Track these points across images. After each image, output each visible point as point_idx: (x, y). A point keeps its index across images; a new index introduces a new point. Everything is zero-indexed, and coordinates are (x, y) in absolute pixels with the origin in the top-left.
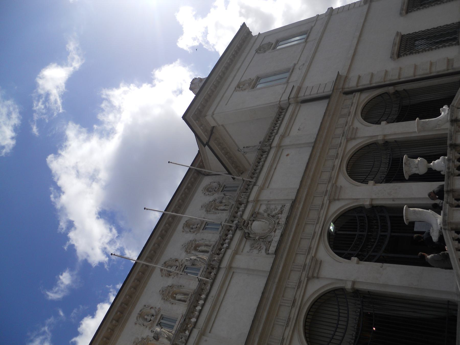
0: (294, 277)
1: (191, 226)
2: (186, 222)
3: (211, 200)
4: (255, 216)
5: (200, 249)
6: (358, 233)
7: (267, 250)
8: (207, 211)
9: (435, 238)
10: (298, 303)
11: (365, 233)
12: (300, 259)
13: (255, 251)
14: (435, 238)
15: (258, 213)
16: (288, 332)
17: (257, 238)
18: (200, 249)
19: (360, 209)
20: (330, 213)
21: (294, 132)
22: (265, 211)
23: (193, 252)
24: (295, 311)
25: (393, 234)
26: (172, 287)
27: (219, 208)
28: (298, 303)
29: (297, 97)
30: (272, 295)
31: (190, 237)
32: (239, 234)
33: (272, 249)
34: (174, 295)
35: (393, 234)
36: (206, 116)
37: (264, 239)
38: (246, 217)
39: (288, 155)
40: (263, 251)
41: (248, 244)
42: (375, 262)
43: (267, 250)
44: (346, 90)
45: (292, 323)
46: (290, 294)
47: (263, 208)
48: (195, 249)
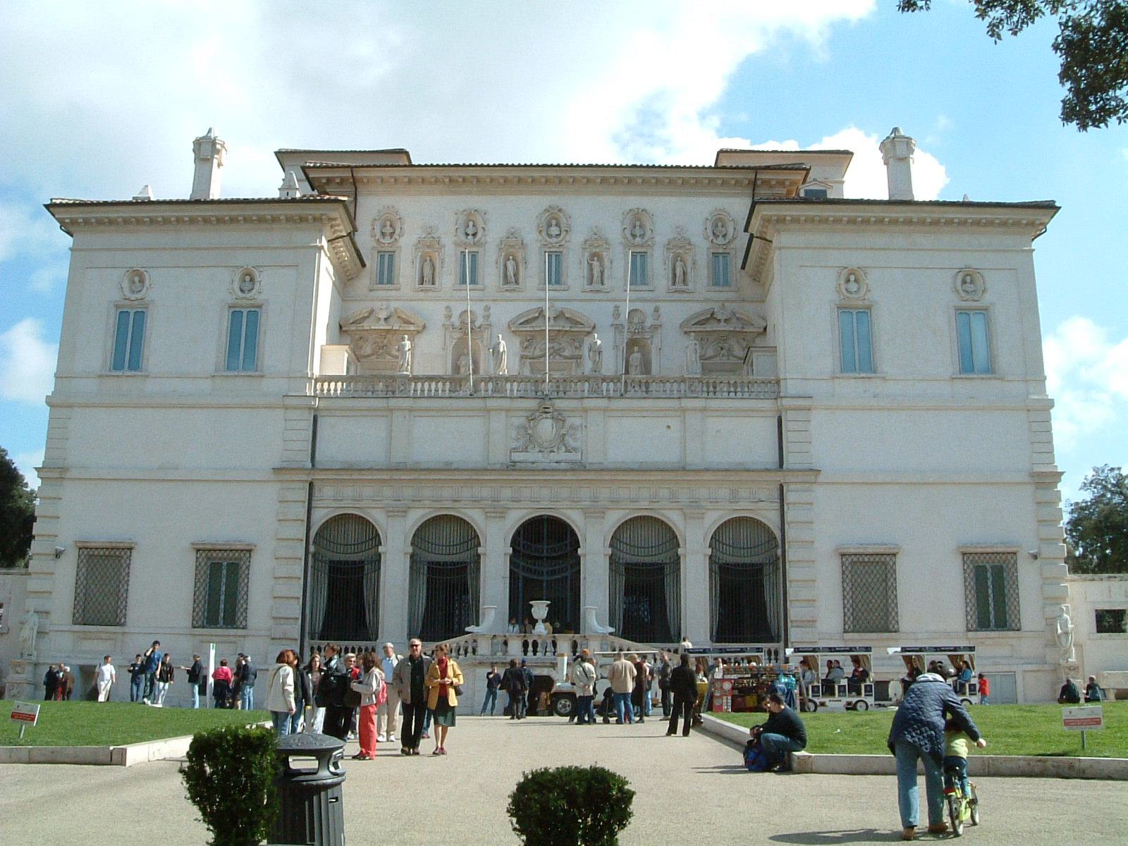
0: (486, 492)
1: (638, 223)
3: (693, 240)
4: (559, 418)
5: (596, 263)
7: (515, 450)
8: (669, 246)
9: (467, 629)
10: (457, 505)
11: (545, 554)
12: (507, 493)
13: (514, 434)
14: (467, 629)
17: (530, 432)
18: (596, 263)
19: (576, 544)
20: (569, 512)
21: (714, 423)
22: (572, 427)
23: (587, 254)
26: (523, 245)
27: (678, 264)
29: (787, 410)
30: (457, 477)
31: (614, 231)
32: (533, 404)
33: (517, 457)
34: (511, 257)
36: (778, 231)
37: (530, 440)
38: (559, 404)
39: (669, 427)
40: (514, 445)
41: (523, 420)
42: (510, 569)
43: (515, 450)
46: (466, 493)
47: (577, 421)
48: (594, 256)
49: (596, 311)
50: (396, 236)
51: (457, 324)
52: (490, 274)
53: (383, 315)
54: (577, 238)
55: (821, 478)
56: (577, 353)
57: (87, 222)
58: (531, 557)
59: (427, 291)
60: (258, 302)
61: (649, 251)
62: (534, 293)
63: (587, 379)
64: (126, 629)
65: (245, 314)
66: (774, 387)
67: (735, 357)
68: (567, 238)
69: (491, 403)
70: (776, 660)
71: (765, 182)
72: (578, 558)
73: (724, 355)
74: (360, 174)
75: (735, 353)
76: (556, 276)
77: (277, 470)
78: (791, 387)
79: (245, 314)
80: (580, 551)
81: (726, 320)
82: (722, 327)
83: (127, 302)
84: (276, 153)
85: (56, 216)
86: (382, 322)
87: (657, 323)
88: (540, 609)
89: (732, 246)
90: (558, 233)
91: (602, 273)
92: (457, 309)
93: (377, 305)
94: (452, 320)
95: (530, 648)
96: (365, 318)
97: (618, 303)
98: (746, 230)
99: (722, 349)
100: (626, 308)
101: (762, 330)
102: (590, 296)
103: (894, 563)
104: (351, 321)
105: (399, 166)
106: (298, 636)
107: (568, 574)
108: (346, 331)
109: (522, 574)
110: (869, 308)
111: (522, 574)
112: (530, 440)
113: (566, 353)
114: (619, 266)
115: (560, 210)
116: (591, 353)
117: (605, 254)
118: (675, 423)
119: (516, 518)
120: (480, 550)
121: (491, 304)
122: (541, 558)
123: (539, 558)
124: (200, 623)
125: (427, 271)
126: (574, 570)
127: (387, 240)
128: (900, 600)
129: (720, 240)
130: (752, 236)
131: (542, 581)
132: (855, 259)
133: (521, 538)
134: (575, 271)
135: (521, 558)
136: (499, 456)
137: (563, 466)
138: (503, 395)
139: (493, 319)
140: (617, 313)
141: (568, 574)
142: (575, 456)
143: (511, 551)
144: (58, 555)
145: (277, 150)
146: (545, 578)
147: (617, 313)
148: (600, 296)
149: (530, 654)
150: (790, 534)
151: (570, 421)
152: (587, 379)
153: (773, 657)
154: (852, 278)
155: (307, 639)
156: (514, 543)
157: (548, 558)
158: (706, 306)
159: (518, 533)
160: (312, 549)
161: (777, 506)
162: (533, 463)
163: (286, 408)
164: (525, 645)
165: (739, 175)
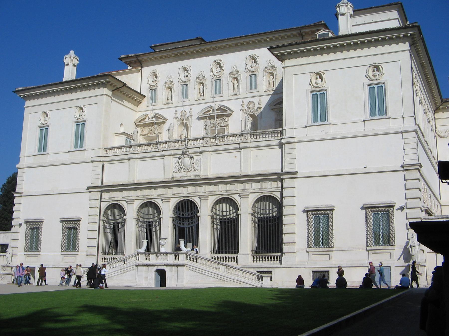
11: (186, 216)
13: (174, 165)
15: (193, 158)
16: (141, 197)
19: (198, 211)
24: (149, 197)
25: (186, 229)
33: (175, 175)
38: (190, 150)
39: (236, 157)
51: (179, 117)
53: (151, 117)
54: (226, 72)
55: (298, 175)
56: (226, 124)
61: (257, 73)
64: (41, 253)
65: (80, 125)
66: (282, 133)
69: (165, 153)
71: (307, 33)
72: (198, 217)
74: (140, 58)
76: (218, 90)
77: (89, 188)
78: (287, 134)
79: (80, 125)
83: (42, 125)
86: (151, 119)
91: (238, 86)
96: (145, 118)
100: (246, 101)
102: (233, 97)
103: (332, 214)
105: (215, 41)
106: (96, 254)
110: (326, 90)
112: (180, 166)
113: (222, 125)
115: (220, 60)
117: (238, 78)
118: (238, 154)
122: (185, 218)
123: (183, 218)
125: (170, 95)
127: (154, 84)
128: (334, 232)
132: (318, 68)
134: (227, 86)
136: (169, 176)
137: (192, 178)
141: (196, 223)
142: (196, 173)
143: (173, 215)
144: (20, 225)
148: (237, 97)
150: (286, 201)
151: (194, 157)
154: (318, 77)
155: (100, 254)
157: (187, 218)
160: (102, 218)
161: (280, 189)
163: (92, 162)
165: (294, 33)
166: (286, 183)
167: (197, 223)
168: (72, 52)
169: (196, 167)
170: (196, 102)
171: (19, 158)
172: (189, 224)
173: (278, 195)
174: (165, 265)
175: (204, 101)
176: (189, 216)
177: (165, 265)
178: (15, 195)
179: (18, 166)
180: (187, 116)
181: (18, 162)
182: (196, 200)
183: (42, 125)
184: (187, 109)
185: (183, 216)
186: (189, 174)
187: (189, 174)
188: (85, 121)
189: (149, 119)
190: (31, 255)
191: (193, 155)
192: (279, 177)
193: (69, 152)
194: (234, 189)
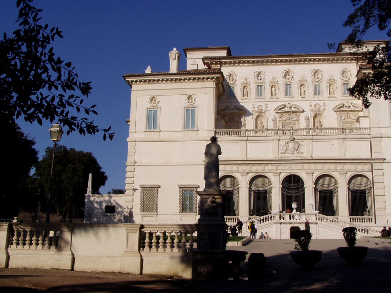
0: (273, 167)
2: (318, 69)
6: (293, 185)
7: (282, 153)
8: (328, 81)
10: (263, 171)
11: (293, 187)
23: (299, 85)
24: (261, 171)
25: (293, 197)
28: (263, 171)
32: (288, 138)
35: (293, 197)
39: (333, 145)
43: (282, 153)
44: (373, 164)
45: (257, 171)
48: (301, 85)
49: (304, 105)
50: (234, 81)
51: (257, 110)
52: (267, 92)
57: (136, 81)
58: (288, 188)
59: (246, 99)
60: (195, 106)
62: (282, 99)
63: (305, 129)
67: (352, 119)
68: (293, 80)
70: (372, 222)
73: (348, 118)
75: (352, 118)
80: (304, 186)
81: (349, 107)
82: (347, 109)
84: (184, 50)
85: (126, 80)
87: (325, 108)
88: (294, 205)
89: (349, 81)
90: (289, 78)
92: (257, 105)
93: (229, 104)
94: (255, 109)
95: (292, 218)
96: (226, 109)
97: (311, 102)
98: (356, 77)
99: (347, 116)
100: (313, 103)
101: (361, 110)
102: (301, 99)
104: (221, 110)
107: (301, 193)
108: (220, 114)
109: (285, 194)
111: (285, 194)
113: (294, 119)
114: (310, 88)
116: (306, 120)
119: (283, 175)
120: (272, 186)
121: (267, 103)
122: (292, 188)
124: (181, 211)
126: (302, 193)
129: (345, 79)
130: (358, 78)
131: (292, 196)
133: (285, 182)
135: (285, 189)
137: (298, 158)
138: (277, 135)
139: (268, 109)
140: (311, 105)
141: (301, 193)
143: (281, 186)
145: (184, 48)
146: (293, 195)
147: (311, 105)
148: (305, 99)
149: (292, 219)
152: (305, 129)
153: (370, 221)
156: (282, 183)
157: (294, 188)
158: (342, 102)
159: (284, 180)
162: (288, 157)
164: (290, 217)
166: (375, 166)
167: (303, 192)
168: (175, 49)
169: (301, 151)
170: (271, 100)
171: (129, 133)
172: (296, 193)
173: (369, 175)
174: (300, 223)
175: (278, 100)
176: (296, 187)
177: (300, 223)
178: (127, 164)
179: (128, 140)
180: (263, 110)
181: (127, 135)
182: (303, 176)
183: (151, 107)
184: (263, 104)
185: (290, 187)
186: (295, 155)
187: (295, 155)
188: (195, 107)
189: (230, 109)
190: (147, 215)
191: (298, 141)
192: (370, 161)
193: (182, 131)
194: (334, 168)
